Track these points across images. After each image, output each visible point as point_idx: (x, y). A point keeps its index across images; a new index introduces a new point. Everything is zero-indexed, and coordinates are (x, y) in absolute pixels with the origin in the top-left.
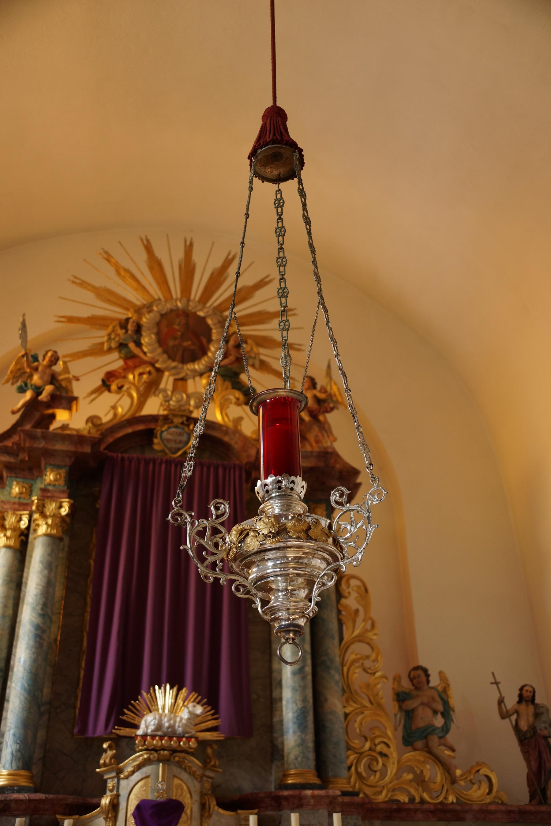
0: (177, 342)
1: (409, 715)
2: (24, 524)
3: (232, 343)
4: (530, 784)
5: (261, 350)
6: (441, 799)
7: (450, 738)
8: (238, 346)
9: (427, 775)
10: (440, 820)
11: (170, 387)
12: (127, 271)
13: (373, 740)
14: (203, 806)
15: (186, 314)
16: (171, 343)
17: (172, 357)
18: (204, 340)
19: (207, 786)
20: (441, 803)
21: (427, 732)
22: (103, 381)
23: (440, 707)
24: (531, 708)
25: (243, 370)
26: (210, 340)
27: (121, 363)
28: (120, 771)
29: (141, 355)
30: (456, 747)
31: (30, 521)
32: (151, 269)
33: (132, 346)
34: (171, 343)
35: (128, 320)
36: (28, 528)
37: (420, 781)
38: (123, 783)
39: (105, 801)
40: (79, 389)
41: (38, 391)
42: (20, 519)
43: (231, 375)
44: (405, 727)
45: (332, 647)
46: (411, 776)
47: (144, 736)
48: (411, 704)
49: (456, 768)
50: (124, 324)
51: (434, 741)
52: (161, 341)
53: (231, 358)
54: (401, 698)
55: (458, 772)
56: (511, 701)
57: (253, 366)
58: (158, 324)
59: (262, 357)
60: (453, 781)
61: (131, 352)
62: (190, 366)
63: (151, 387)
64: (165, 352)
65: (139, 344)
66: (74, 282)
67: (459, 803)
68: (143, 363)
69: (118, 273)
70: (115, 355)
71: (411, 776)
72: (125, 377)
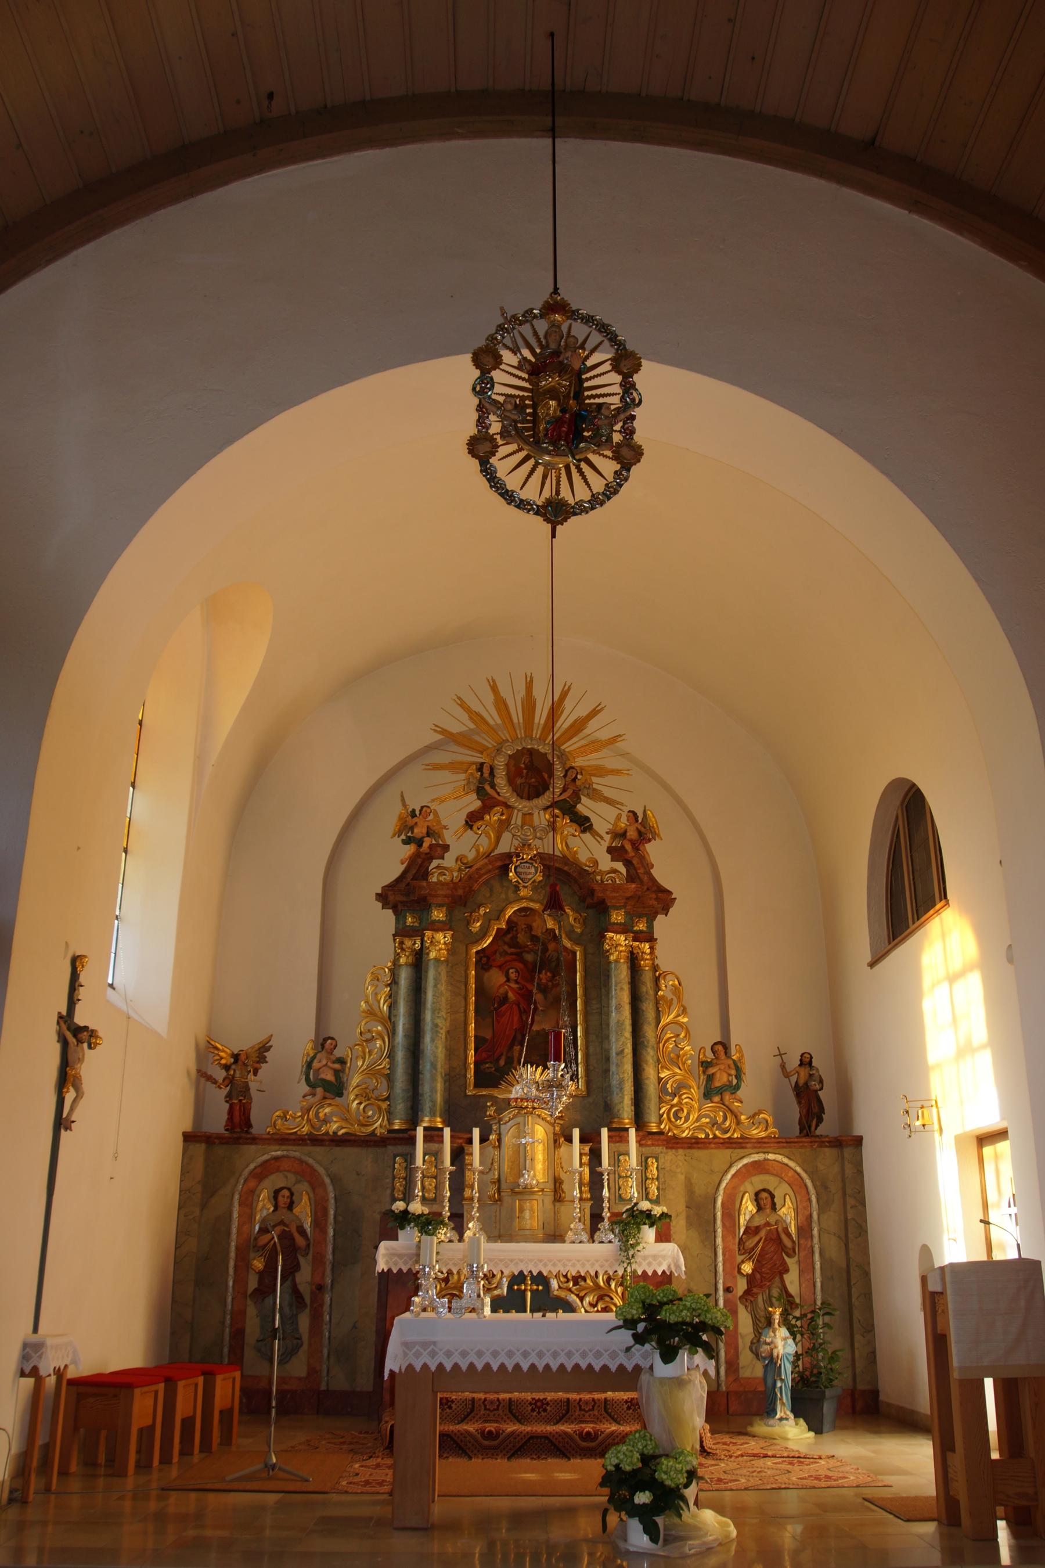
0: (523, 780)
1: (710, 1078)
2: (417, 946)
3: (568, 779)
4: (800, 1123)
5: (594, 779)
6: (728, 1135)
7: (740, 1093)
8: (575, 779)
9: (720, 1119)
10: (728, 1148)
11: (519, 822)
12: (478, 714)
13: (680, 1096)
14: (555, 1141)
15: (531, 752)
16: (519, 781)
17: (520, 796)
18: (546, 776)
19: (557, 1129)
20: (729, 1138)
21: (720, 1091)
22: (466, 822)
23: (733, 1072)
24: (808, 1069)
25: (579, 800)
26: (551, 775)
27: (479, 803)
28: (500, 1120)
29: (496, 796)
30: (743, 1100)
31: (422, 944)
32: (498, 710)
33: (487, 787)
34: (519, 781)
35: (482, 764)
36: (421, 949)
37: (714, 1123)
38: (503, 1127)
39: (493, 1137)
40: (448, 837)
41: (420, 843)
42: (415, 943)
43: (568, 809)
44: (706, 1086)
45: (649, 1032)
46: (708, 1120)
47: (516, 1100)
48: (711, 1071)
49: (742, 1114)
50: (480, 767)
51: (727, 1097)
52: (511, 782)
53: (569, 792)
54: (705, 1065)
55: (743, 1117)
56: (793, 1062)
57: (588, 796)
58: (507, 765)
59: (595, 786)
60: (738, 1122)
61: (487, 794)
62: (535, 801)
63: (504, 825)
64: (514, 790)
65: (493, 786)
66: (435, 731)
67: (742, 1137)
68: (498, 803)
69: (471, 718)
70: (474, 796)
71: (708, 1120)
72: (483, 818)
